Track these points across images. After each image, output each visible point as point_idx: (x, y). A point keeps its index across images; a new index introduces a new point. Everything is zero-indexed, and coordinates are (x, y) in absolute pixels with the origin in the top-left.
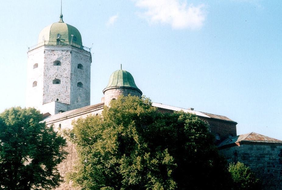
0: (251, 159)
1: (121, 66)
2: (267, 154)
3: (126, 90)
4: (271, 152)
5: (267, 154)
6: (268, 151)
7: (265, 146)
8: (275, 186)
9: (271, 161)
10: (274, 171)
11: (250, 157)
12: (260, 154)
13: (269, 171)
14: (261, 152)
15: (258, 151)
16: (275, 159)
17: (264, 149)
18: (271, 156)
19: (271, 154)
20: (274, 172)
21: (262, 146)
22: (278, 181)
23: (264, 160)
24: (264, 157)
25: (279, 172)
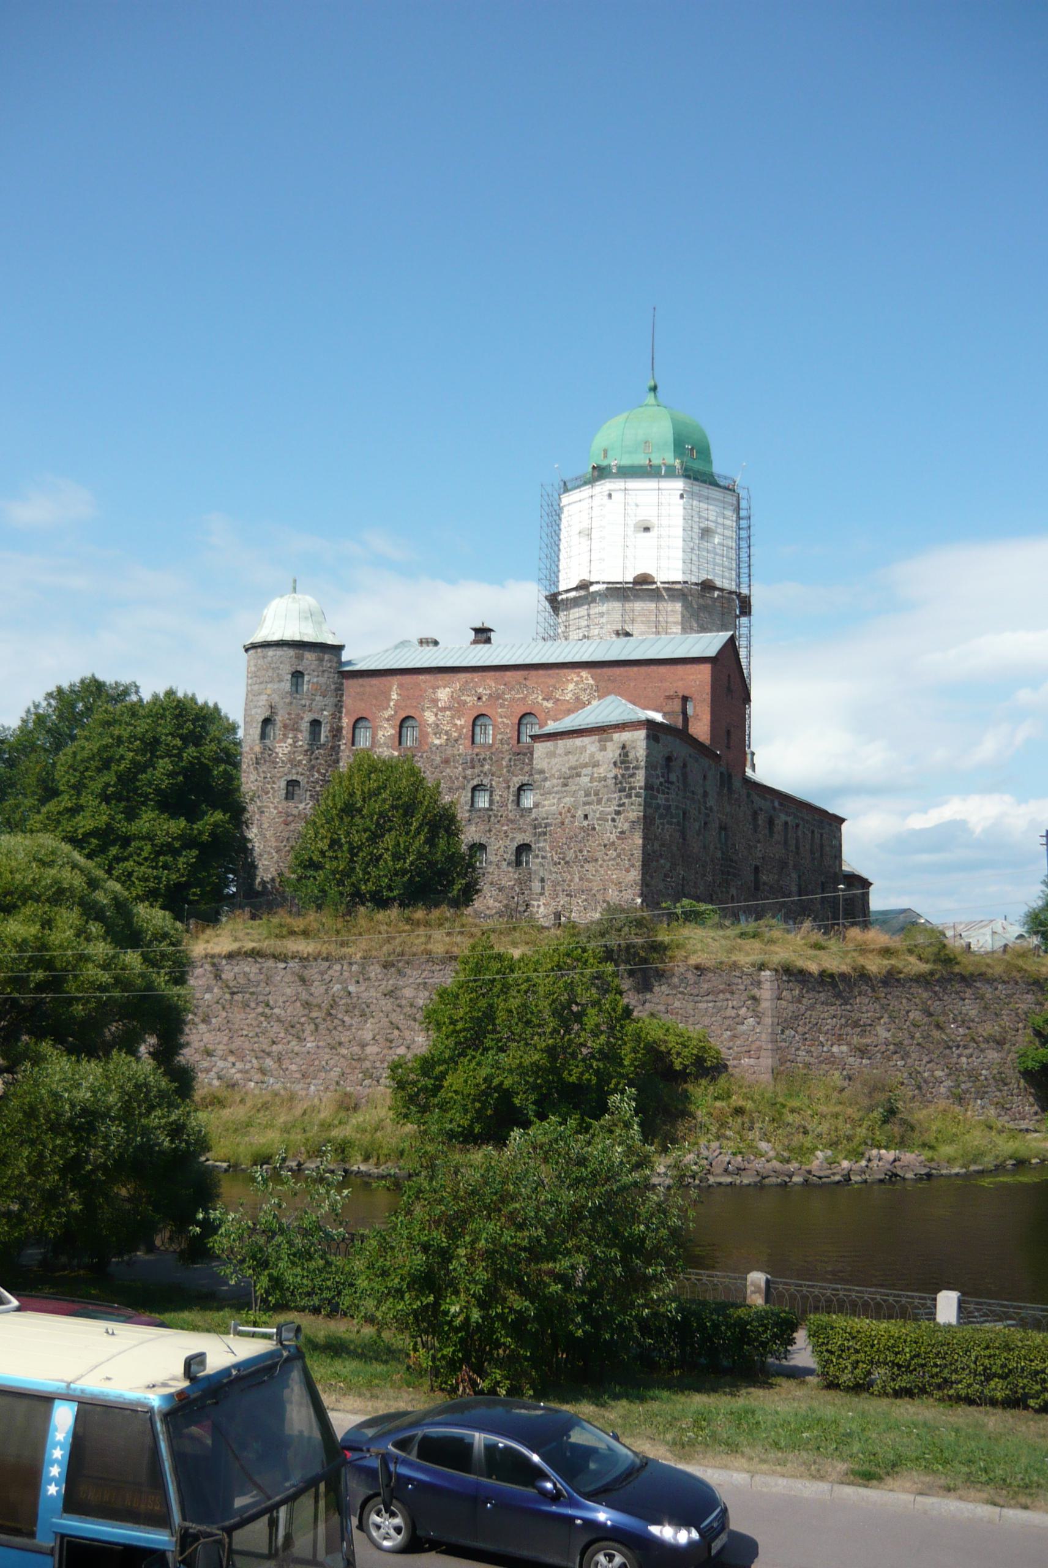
0: (548, 784)
1: (292, 584)
2: (585, 766)
3: (259, 650)
4: (599, 756)
5: (585, 766)
6: (592, 756)
7: (586, 740)
8: (596, 860)
9: (596, 784)
10: (598, 815)
11: (546, 779)
12: (570, 768)
13: (586, 816)
14: (572, 760)
15: (566, 758)
16: (605, 779)
17: (583, 748)
18: (595, 769)
19: (596, 765)
20: (598, 819)
21: (578, 742)
22: (605, 846)
23: (578, 784)
24: (579, 775)
25: (609, 817)
